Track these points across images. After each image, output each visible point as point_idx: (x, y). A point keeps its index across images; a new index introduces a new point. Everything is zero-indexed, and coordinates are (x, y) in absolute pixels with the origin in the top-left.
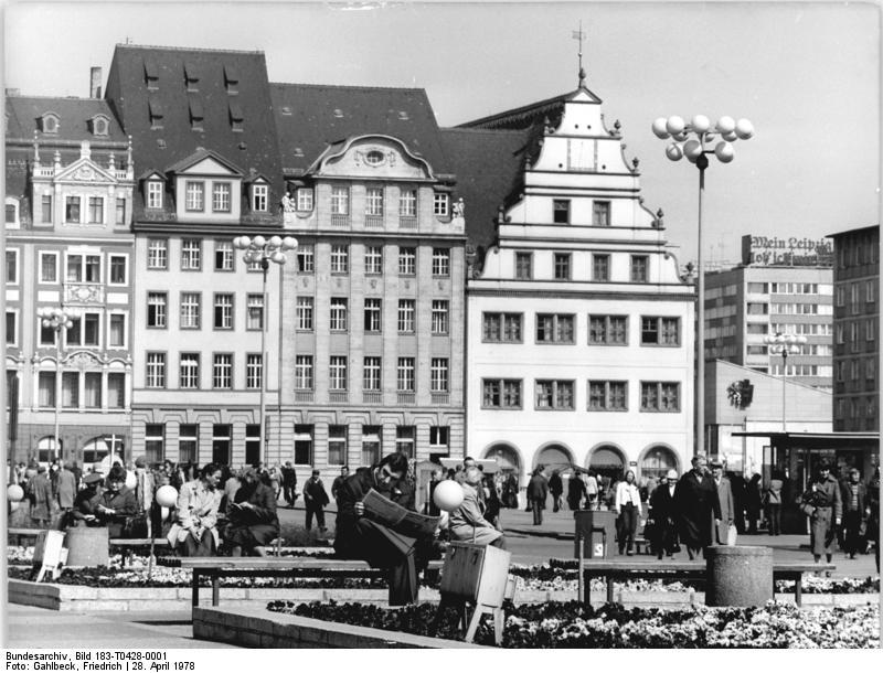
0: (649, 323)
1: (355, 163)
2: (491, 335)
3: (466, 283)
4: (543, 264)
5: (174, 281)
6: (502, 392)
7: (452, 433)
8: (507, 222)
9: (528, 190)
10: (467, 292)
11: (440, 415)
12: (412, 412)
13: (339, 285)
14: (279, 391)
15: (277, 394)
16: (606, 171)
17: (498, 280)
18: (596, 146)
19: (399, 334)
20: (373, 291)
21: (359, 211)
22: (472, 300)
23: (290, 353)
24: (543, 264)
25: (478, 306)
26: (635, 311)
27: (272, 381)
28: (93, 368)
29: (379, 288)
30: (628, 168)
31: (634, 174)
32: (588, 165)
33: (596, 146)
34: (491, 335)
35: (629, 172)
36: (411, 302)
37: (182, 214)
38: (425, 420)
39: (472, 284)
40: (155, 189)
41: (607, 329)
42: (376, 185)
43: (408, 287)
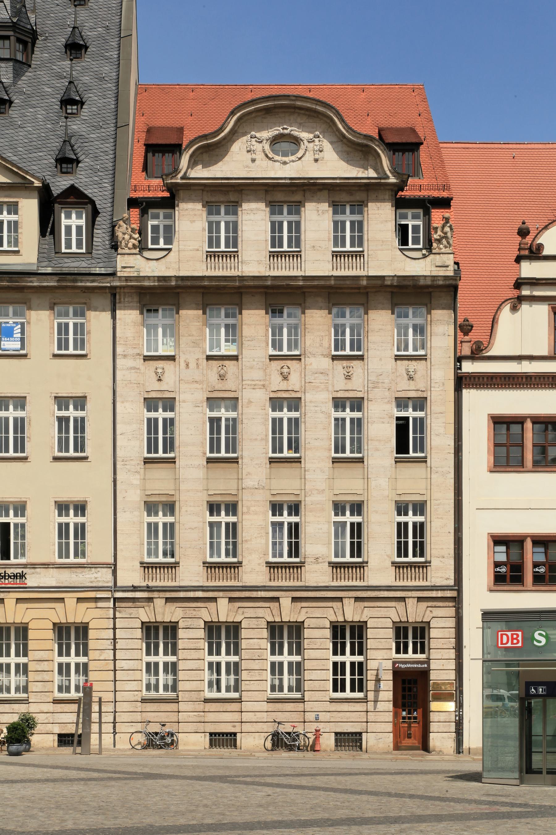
1: (249, 156)
7: (434, 633)
11: (411, 603)
12: (357, 599)
13: (222, 377)
14: (114, 568)
15: (110, 571)
19: (335, 461)
20: (284, 385)
22: (466, 393)
23: (132, 496)
27: (98, 548)
36: (357, 404)
43: (348, 377)
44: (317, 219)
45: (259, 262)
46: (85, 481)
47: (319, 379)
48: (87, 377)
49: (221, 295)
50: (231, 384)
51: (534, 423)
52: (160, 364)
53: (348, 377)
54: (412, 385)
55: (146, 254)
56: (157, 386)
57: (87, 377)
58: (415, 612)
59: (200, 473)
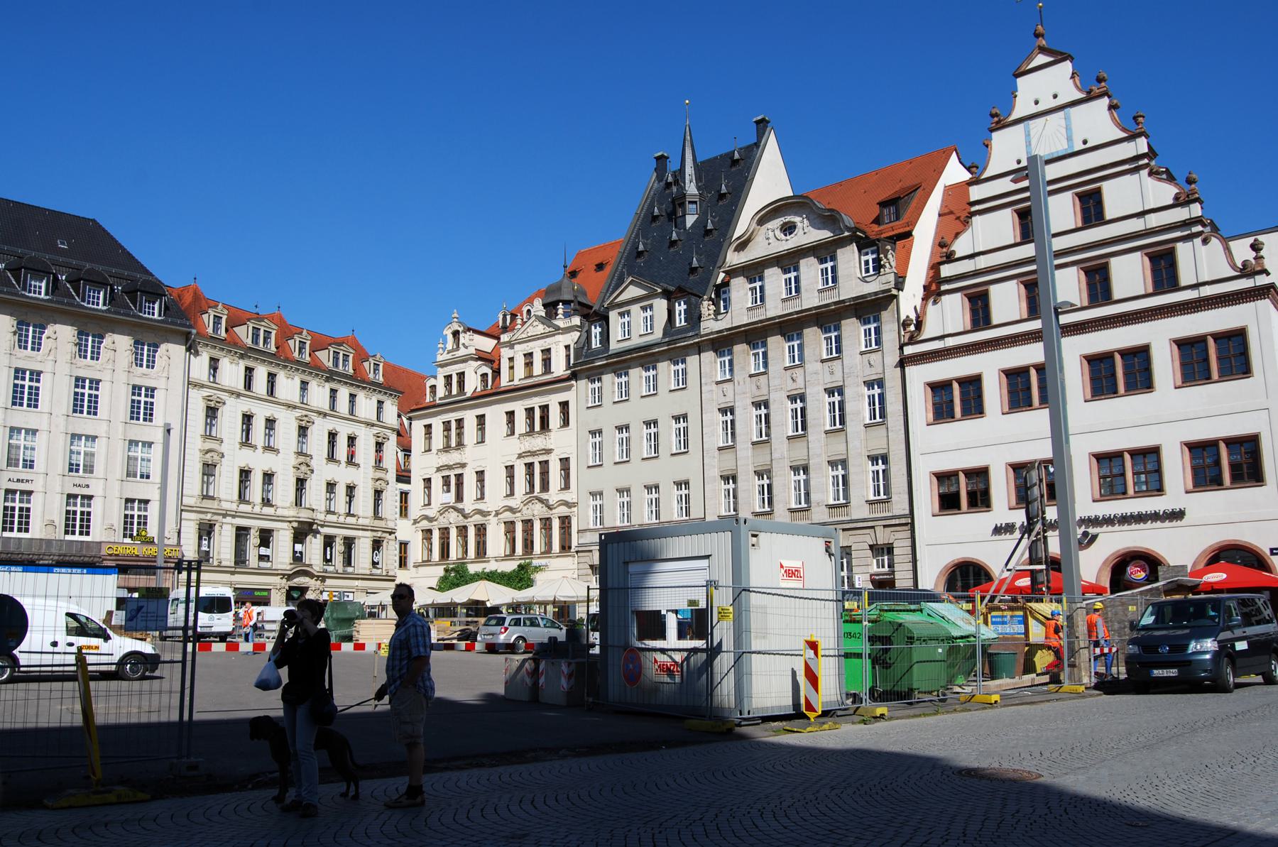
0: (1190, 348)
2: (942, 412)
3: (901, 348)
4: (1007, 302)
5: (608, 417)
6: (963, 492)
8: (950, 258)
9: (973, 209)
10: (903, 363)
11: (879, 530)
12: (844, 530)
16: (1088, 146)
17: (942, 338)
18: (1067, 118)
21: (776, 295)
22: (911, 371)
23: (714, 473)
24: (1007, 302)
25: (920, 376)
26: (1160, 337)
28: (545, 512)
29: (800, 382)
30: (1124, 130)
31: (1132, 137)
32: (1061, 147)
33: (1067, 118)
34: (942, 412)
35: (1124, 135)
37: (614, 346)
38: (861, 538)
39: (909, 350)
40: (596, 331)
41: (1121, 374)
42: (788, 261)
43: (832, 373)
44: (810, 270)
45: (776, 307)
46: (688, 467)
47: (816, 378)
48: (686, 402)
49: (755, 335)
50: (765, 391)
51: (960, 384)
52: (725, 385)
53: (832, 373)
54: (873, 371)
55: (720, 317)
56: (723, 400)
57: (686, 402)
58: (883, 537)
59: (750, 451)
